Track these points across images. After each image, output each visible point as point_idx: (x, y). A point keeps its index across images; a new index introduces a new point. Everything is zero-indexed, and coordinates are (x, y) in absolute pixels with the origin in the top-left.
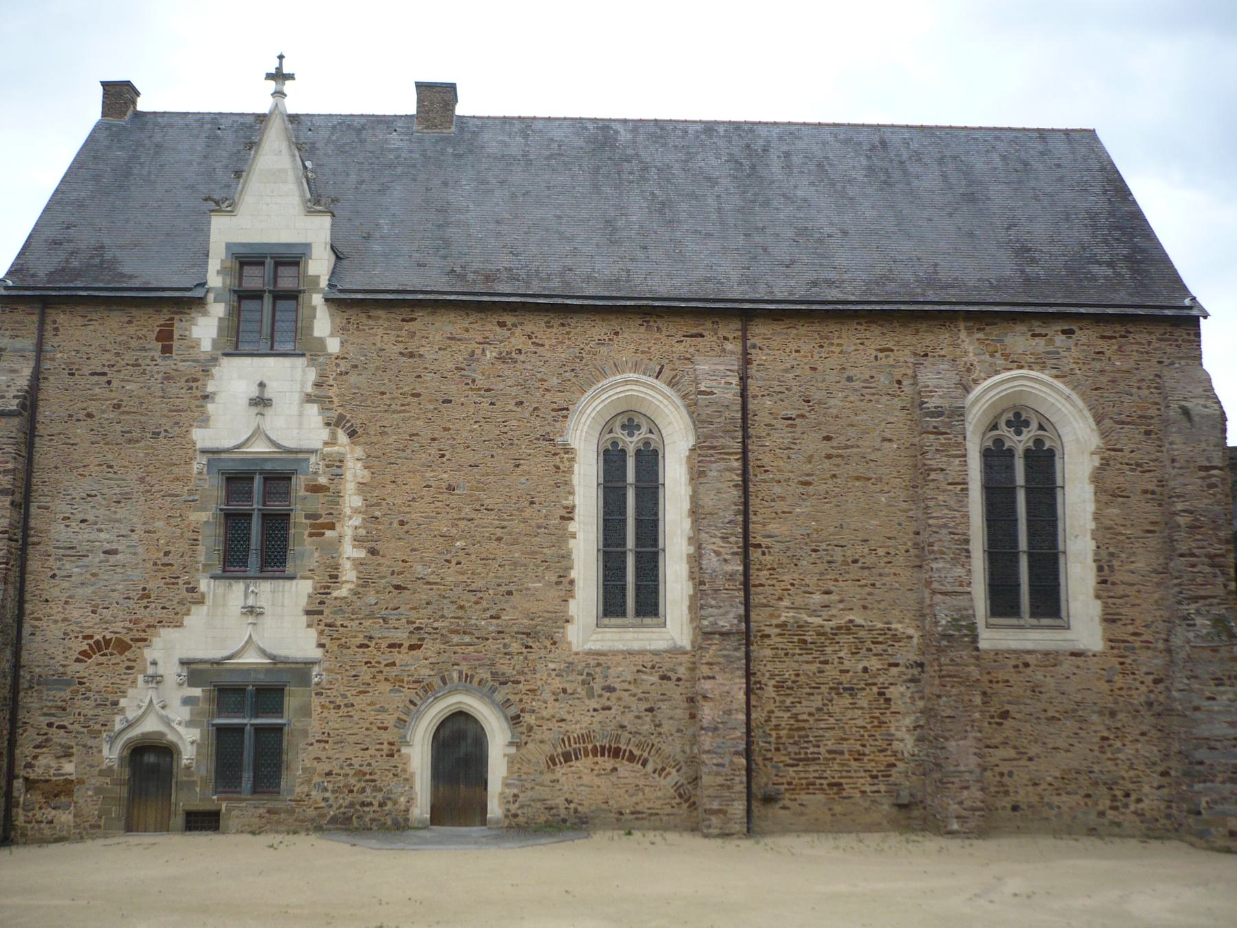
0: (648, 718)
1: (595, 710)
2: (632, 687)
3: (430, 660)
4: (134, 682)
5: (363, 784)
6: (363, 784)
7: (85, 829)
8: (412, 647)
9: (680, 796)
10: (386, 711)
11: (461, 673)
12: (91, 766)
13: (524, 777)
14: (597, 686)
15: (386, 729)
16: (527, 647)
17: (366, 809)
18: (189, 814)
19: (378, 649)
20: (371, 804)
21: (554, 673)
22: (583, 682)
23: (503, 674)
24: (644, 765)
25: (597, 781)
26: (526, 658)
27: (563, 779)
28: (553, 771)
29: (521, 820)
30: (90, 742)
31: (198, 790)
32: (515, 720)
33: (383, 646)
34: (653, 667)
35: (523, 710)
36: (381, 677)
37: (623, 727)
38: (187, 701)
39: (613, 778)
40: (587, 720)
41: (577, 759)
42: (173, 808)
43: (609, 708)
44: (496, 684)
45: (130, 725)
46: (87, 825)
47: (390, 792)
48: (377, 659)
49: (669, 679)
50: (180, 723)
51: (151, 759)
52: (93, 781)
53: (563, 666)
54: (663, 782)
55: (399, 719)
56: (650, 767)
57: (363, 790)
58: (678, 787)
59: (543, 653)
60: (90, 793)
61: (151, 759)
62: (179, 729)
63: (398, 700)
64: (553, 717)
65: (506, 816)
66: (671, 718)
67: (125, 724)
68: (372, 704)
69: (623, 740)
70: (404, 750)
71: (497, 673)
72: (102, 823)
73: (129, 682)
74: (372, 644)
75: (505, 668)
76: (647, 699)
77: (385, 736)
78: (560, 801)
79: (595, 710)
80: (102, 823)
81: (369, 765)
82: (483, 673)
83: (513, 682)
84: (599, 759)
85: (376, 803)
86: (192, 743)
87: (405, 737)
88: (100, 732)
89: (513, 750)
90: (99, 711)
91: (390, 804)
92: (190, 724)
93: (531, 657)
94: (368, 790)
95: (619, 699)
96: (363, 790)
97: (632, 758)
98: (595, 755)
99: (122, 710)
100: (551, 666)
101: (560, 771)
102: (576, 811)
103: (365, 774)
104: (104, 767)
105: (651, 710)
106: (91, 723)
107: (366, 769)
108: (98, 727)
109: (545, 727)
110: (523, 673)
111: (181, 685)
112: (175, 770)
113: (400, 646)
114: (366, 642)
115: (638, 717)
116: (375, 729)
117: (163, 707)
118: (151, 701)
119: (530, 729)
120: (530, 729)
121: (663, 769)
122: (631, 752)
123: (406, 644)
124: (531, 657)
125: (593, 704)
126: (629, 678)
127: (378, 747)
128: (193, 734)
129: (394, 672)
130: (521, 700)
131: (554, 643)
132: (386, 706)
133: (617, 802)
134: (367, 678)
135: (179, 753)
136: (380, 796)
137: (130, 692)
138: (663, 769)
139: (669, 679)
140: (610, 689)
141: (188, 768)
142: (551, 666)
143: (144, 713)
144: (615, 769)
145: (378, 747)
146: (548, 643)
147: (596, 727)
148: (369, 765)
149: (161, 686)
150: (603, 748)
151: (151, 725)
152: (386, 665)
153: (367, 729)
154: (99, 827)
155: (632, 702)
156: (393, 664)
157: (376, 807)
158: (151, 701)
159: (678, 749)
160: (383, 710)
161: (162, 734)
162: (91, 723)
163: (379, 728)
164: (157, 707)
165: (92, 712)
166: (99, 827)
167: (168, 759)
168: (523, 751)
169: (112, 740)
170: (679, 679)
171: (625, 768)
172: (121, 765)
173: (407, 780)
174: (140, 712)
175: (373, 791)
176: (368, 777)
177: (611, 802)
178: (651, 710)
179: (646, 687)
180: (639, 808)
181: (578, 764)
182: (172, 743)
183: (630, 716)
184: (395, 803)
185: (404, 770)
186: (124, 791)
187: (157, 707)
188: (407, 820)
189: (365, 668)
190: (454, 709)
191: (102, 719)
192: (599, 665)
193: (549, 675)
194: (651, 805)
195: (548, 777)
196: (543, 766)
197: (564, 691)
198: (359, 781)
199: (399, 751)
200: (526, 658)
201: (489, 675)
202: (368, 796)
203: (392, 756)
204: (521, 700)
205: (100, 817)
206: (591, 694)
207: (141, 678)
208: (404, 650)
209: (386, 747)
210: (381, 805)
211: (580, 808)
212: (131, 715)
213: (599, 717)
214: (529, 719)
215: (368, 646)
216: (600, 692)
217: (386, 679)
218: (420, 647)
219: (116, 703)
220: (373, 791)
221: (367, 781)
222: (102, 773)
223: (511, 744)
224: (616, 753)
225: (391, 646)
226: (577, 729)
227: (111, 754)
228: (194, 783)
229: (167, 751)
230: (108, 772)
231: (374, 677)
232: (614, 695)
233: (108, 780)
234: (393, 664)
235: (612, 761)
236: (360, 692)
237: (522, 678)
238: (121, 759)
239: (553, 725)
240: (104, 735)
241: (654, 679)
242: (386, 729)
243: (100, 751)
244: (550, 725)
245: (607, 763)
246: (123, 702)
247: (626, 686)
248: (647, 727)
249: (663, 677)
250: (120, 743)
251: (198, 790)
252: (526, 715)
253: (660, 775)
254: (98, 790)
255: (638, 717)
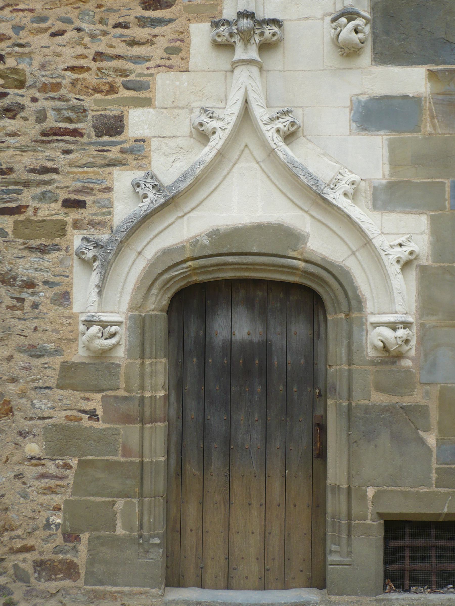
4: (177, 50)
7: (20, 576)
12: (35, 352)
18: (394, 528)
30: (26, 266)
31: (431, 439)
38: (374, 114)
42: (335, 505)
45: (172, 201)
46: (26, 562)
50: (353, 196)
51: (237, 327)
52: (43, 405)
60: (33, 448)
61: (237, 327)
62: (358, 212)
67: (153, 198)
72: (81, 557)
73: (157, 52)
80: (81, 557)
86: (406, 265)
88: (61, 229)
90: (52, 155)
92: (391, 196)
99: (138, 151)
104: (79, 354)
106: (26, 197)
108: (50, 211)
111: (349, 52)
112: (336, 366)
117: (289, 137)
118: (246, 112)
128: (404, 234)
135: (353, 302)
137: (165, 85)
141: (390, 356)
143: (221, 155)
149: (274, 61)
151: (243, 203)
154: (70, 570)
158: (246, 112)
161: (288, 236)
162: (26, 197)
164: (270, 134)
165: (28, 160)
166: (70, 570)
167: (299, 330)
169: (105, 257)
172: (141, 351)
174: (207, 153)
182: (326, 267)
186: (153, 443)
187: (270, 134)
191: (65, 183)
205: (71, 537)
207: (200, 34)
212: (169, 165)
219: (113, 127)
222: (70, 376)
227: (106, 305)
228: (416, 413)
229: (304, 296)
230: (92, 373)
233: (96, 402)
238: (140, 324)
240: (76, 240)
243: (64, 298)
246: (138, 122)
250: (133, 268)
251: (431, 439)
254: (63, 439)
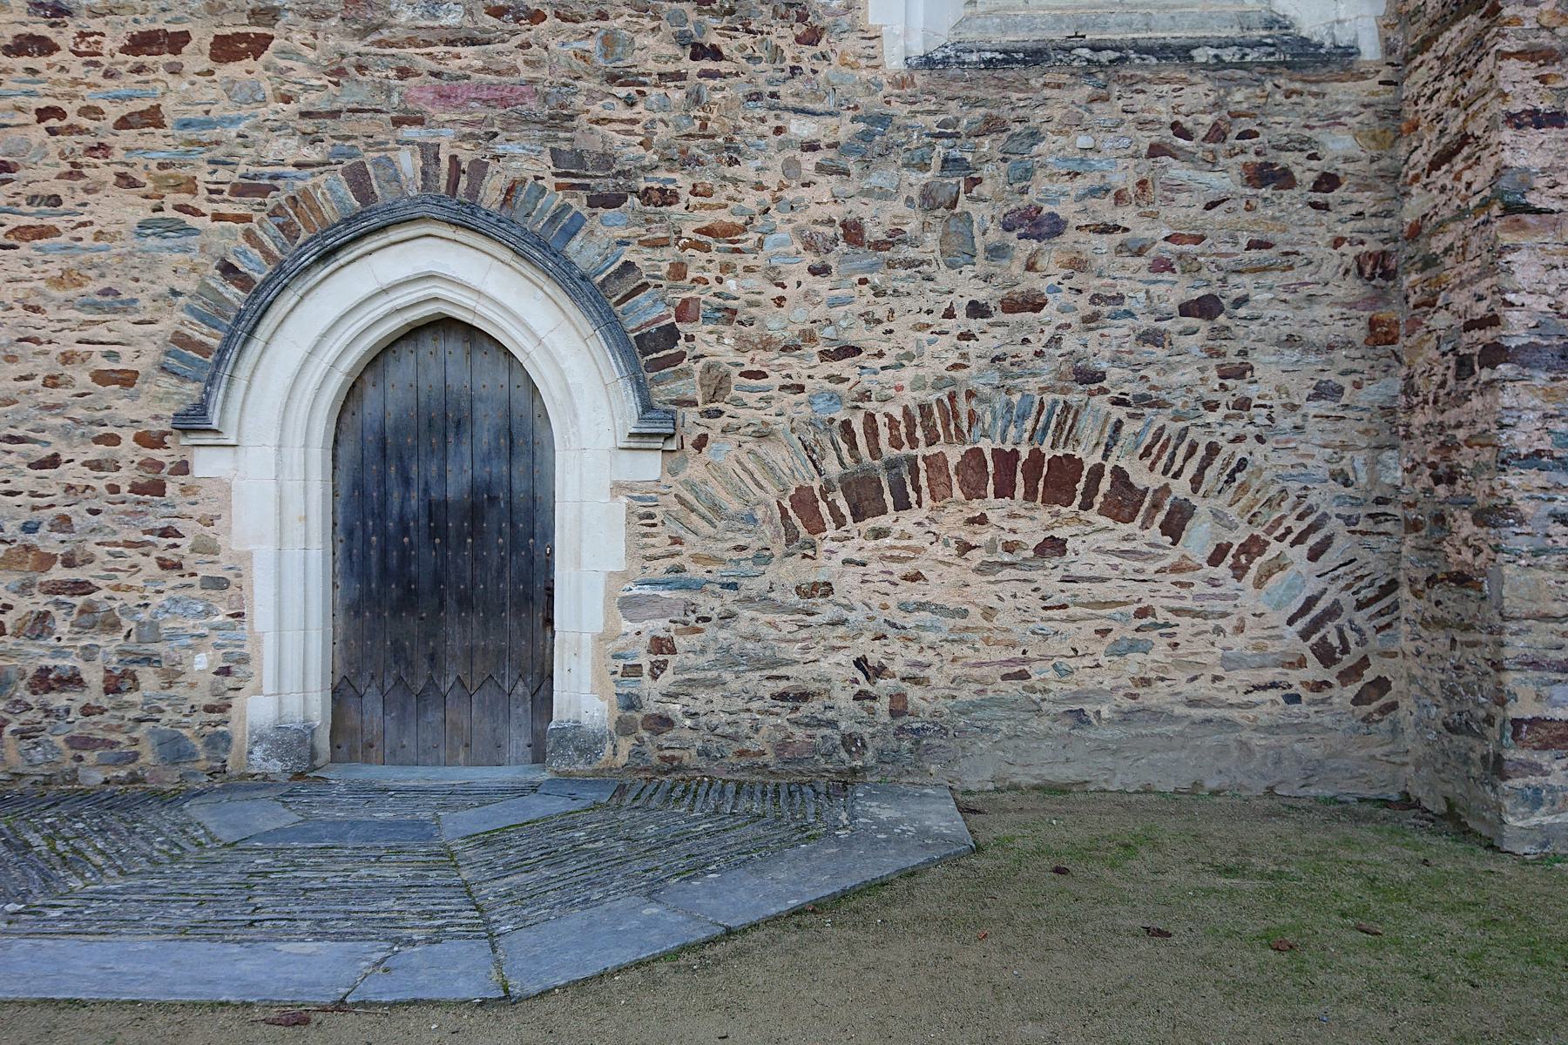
0: (1194, 337)
1: (976, 310)
2: (1126, 215)
3: (305, 101)
5: (41, 602)
6: (41, 602)
8: (225, 49)
9: (1326, 655)
10: (128, 306)
11: (429, 153)
13: (696, 571)
14: (982, 215)
15: (127, 379)
16: (699, 52)
17: (58, 700)
19: (91, 57)
20: (73, 681)
21: (809, 161)
22: (928, 200)
23: (606, 160)
24: (1174, 528)
25: (983, 590)
26: (696, 99)
27: (848, 583)
28: (809, 551)
29: (684, 742)
32: (649, 352)
33: (108, 45)
34: (1217, 134)
35: (684, 311)
36: (104, 172)
37: (1089, 377)
39: (1048, 578)
40: (945, 350)
41: (902, 504)
43: (1034, 304)
44: (578, 203)
47: (152, 631)
48: (91, 98)
49: (1285, 179)
53: (846, 129)
54: (1249, 597)
55: (181, 340)
56: (1199, 537)
57: (40, 625)
58: (1312, 617)
59: (764, 71)
63: (180, 268)
64: (809, 337)
65: (624, 727)
66: (1291, 341)
68: (65, 279)
69: (1089, 431)
70: (207, 463)
71: (579, 158)
74: (64, 38)
75: (614, 129)
76: (1191, 267)
77: (123, 407)
78: (836, 667)
79: (976, 310)
81: (63, 523)
82: (524, 158)
83: (645, 196)
84: (995, 508)
85: (94, 676)
87: (202, 409)
89: (649, 466)
91: (148, 678)
93: (718, 94)
94: (62, 626)
95: (1077, 265)
96: (40, 625)
97: (1125, 501)
98: (974, 491)
100: (800, 128)
101: (840, 551)
102: (899, 707)
103: (47, 561)
105: (1205, 308)
107: (51, 542)
109: (775, 379)
110: (689, 162)
113: (178, 42)
114: (42, 29)
115: (1152, 338)
116: (83, 378)
119: (717, 385)
120: (717, 385)
121: (1254, 547)
122: (1119, 473)
123: (202, 34)
124: (718, 94)
125: (970, 288)
126: (1123, 177)
127: (97, 452)
129: (158, 144)
130: (678, 271)
131: (812, 37)
132: (128, 290)
133: (1063, 673)
134: (44, 175)
136: (109, 645)
138: (1254, 547)
139: (1285, 179)
140: (1039, 225)
142: (800, 128)
144: (1053, 546)
145: (97, 452)
146: (784, 36)
147: (978, 376)
148: (63, 523)
150: (1006, 460)
152: (124, 123)
153: (52, 382)
155: (1132, 280)
156: (152, 118)
157: (94, 693)
159: (1319, 465)
160: (112, 302)
163: (101, 377)
168: (695, 469)
170: (1328, 182)
171: (1094, 539)
173: (219, 584)
175: (81, 628)
176: (58, 573)
177: (1040, 673)
178: (1205, 308)
179: (1184, 211)
180: (1156, 696)
181: (907, 521)
183: (1120, 331)
184: (171, 677)
185: (207, 548)
188: (218, 742)
189: (38, 133)
190: (413, 304)
192: (992, 126)
193: (791, 167)
194: (1203, 688)
195: (789, 572)
196: (769, 534)
197: (852, 231)
198: (24, 589)
199: (183, 468)
200: (696, 99)
201: (544, 166)
202: (64, 646)
203: (158, 488)
204: (678, 271)
206: (959, 253)
208: (195, 58)
209: (128, 448)
210: (113, 686)
211: (914, 694)
213: (991, 339)
214: (710, 344)
215: (46, 47)
216: (995, 236)
217: (125, 181)
218: (259, 45)
220: (81, 628)
221: (55, 589)
223: (640, 439)
224: (1059, 481)
225: (141, 43)
226: (903, 390)
231: (75, 172)
232: (1052, 257)
234: (152, 118)
235: (1043, 515)
236: (24, 233)
237: (682, 182)
239: (810, 368)
241: (1226, 180)
242: (127, 379)
244: (797, 368)
245: (1031, 523)
247: (1105, 211)
248: (1186, 370)
249: (1266, 176)
252: (701, 330)
253: (1239, 571)
255: (1152, 338)
